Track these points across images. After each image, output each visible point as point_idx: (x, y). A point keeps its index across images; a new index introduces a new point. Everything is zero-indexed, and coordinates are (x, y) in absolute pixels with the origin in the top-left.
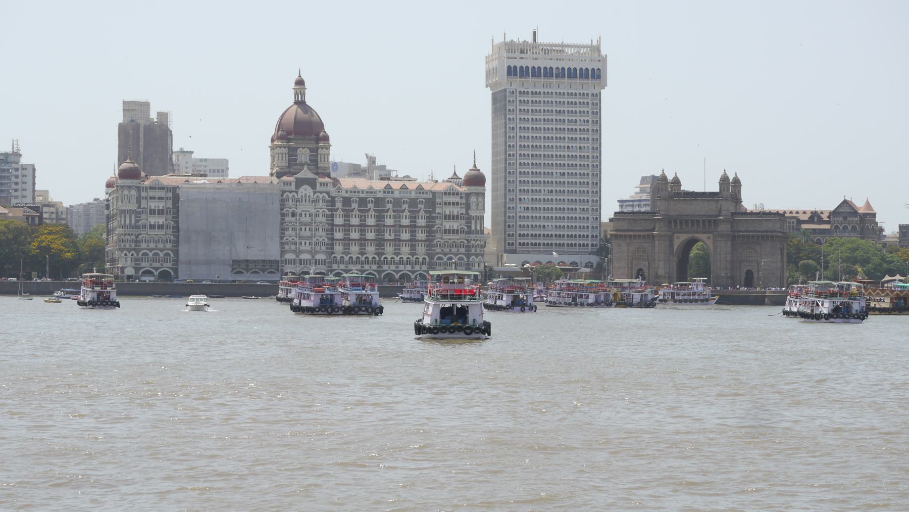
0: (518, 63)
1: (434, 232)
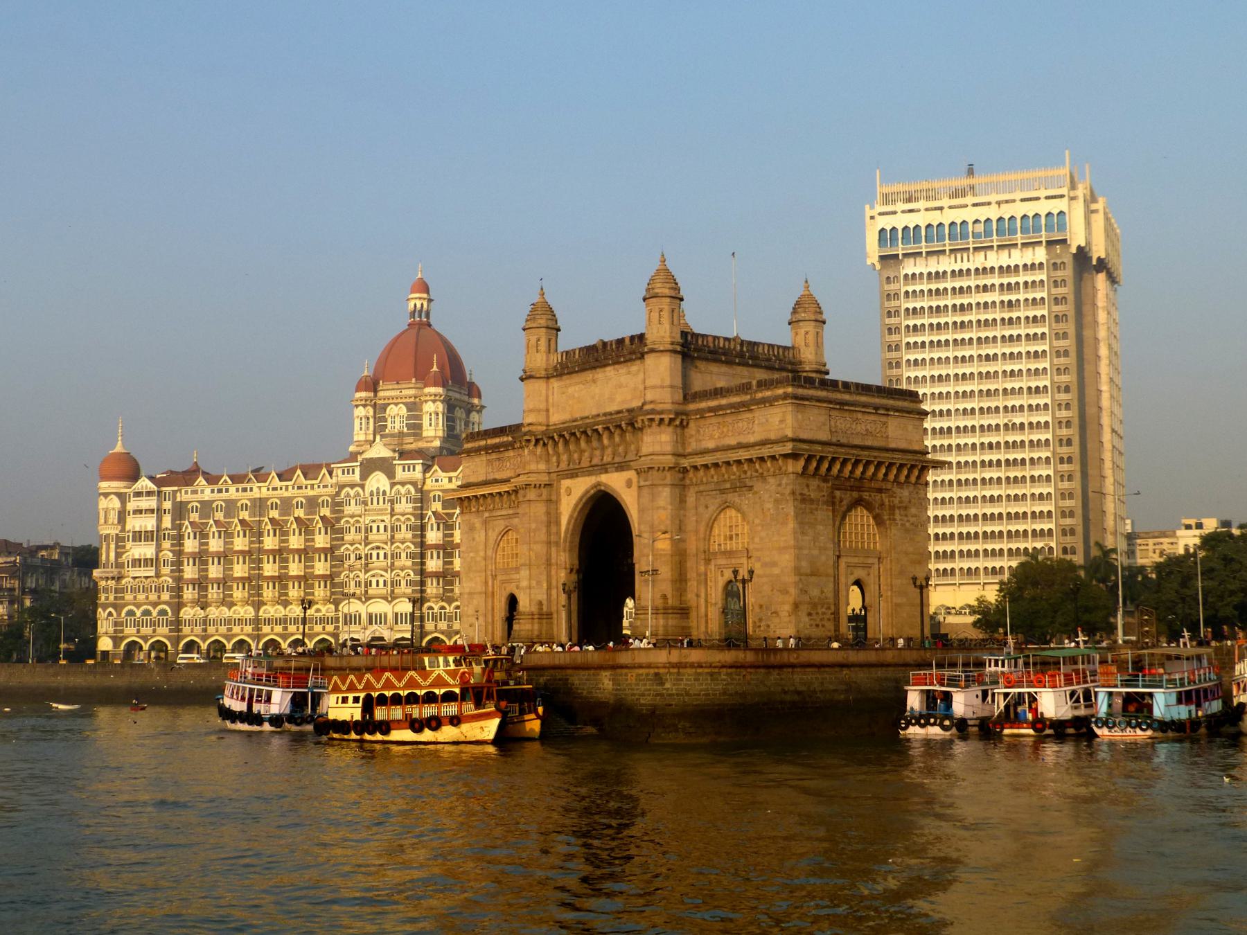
0: (900, 221)
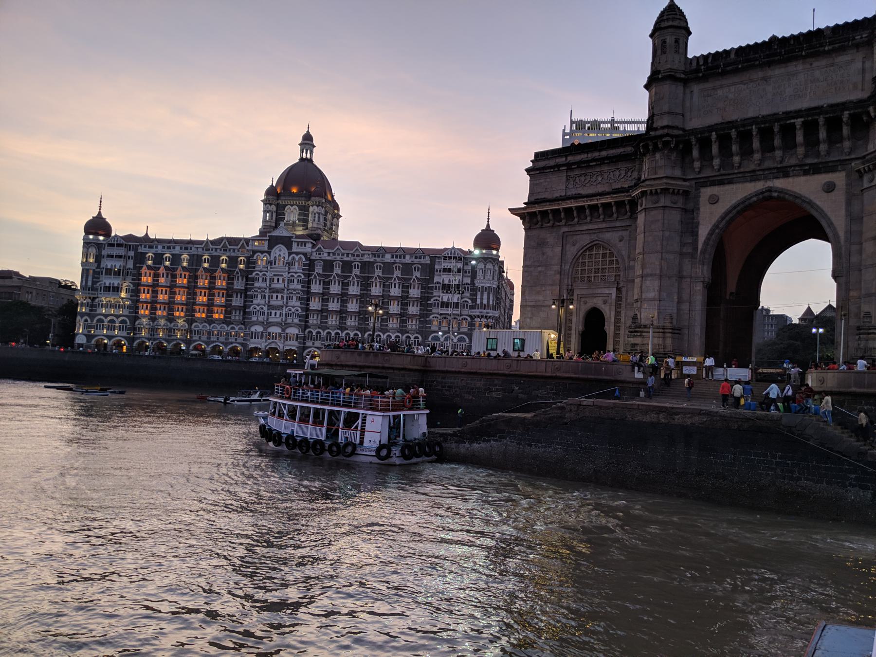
1: (431, 305)
